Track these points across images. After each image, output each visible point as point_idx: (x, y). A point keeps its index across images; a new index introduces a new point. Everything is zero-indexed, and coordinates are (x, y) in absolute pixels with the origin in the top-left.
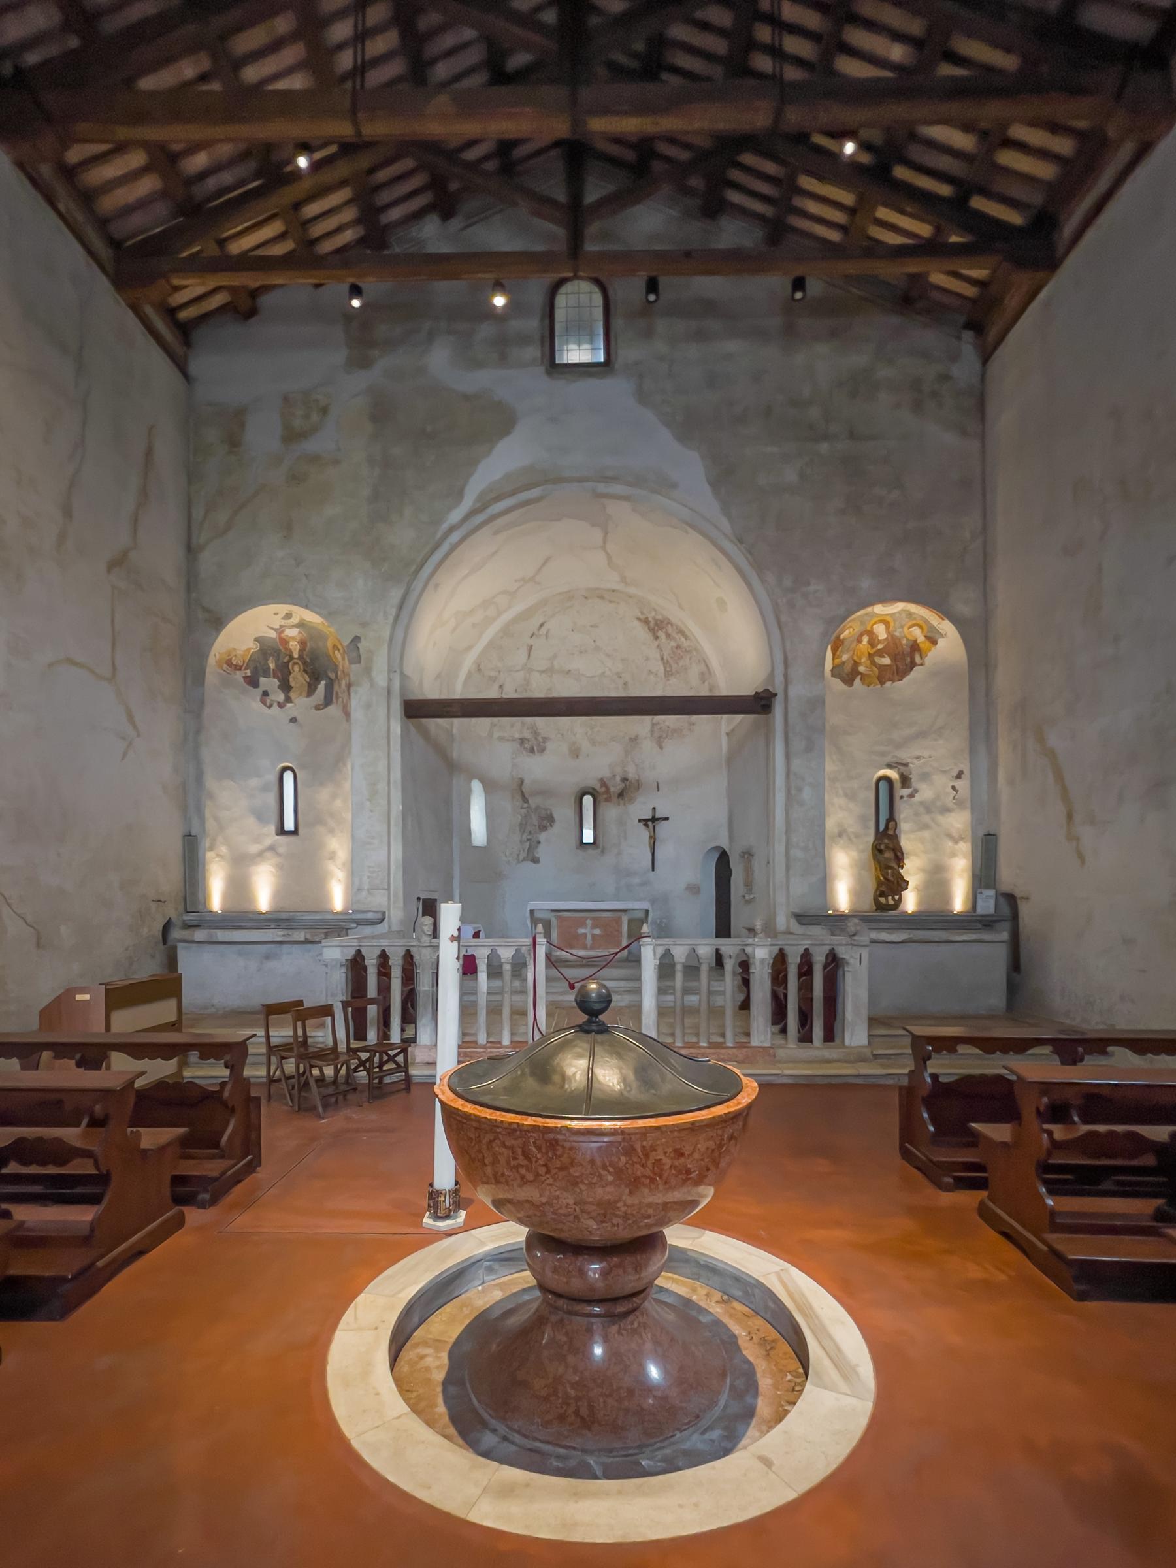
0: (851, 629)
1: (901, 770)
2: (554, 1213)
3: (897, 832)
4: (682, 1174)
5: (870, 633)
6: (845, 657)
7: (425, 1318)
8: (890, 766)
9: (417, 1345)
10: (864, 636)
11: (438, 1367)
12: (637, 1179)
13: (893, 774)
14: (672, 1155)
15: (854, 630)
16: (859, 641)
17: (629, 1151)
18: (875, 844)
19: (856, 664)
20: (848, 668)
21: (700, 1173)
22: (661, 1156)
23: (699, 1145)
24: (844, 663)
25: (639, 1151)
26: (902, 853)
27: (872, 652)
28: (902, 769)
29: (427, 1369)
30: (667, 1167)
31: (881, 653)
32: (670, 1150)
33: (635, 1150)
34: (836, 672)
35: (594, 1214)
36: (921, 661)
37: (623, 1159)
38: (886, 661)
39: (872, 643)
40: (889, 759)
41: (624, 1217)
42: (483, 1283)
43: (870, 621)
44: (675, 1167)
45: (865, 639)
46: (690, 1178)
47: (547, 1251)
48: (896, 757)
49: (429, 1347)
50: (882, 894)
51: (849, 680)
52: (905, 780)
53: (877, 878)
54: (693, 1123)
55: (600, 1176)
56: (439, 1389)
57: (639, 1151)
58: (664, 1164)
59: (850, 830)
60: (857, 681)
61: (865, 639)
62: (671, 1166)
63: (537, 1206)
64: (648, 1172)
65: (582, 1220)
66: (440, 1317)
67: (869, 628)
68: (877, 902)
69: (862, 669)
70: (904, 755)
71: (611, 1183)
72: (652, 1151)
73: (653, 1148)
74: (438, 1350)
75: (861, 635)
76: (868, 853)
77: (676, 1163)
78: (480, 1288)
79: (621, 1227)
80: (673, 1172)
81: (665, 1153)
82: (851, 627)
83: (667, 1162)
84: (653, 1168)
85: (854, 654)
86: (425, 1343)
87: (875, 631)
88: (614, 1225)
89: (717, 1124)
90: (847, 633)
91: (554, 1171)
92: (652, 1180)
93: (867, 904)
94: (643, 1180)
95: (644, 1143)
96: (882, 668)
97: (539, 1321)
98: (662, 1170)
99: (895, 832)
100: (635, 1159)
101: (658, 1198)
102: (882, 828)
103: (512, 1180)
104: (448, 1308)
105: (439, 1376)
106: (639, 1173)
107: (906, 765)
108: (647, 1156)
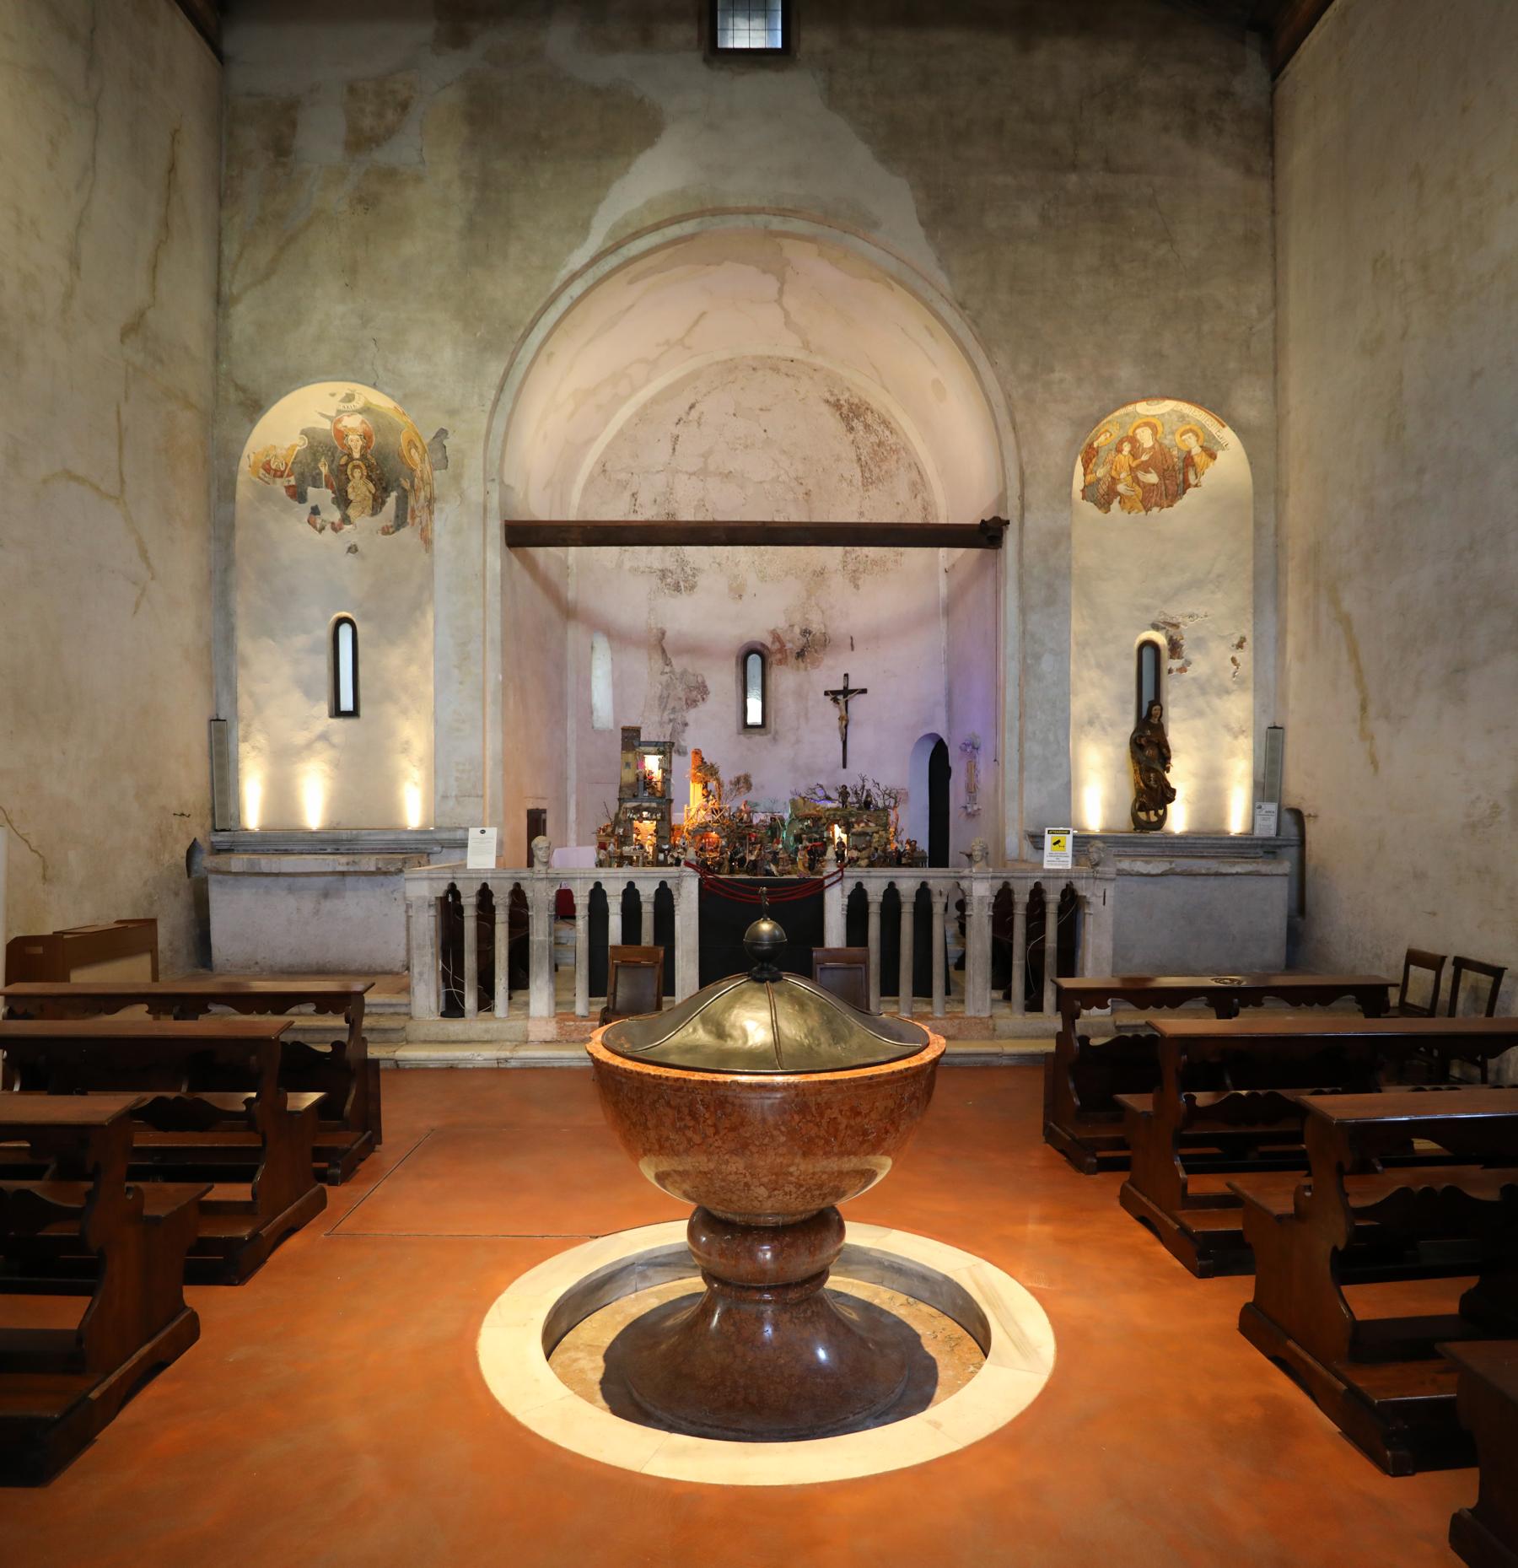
0: (1108, 435)
1: (1170, 633)
2: (723, 1180)
3: (1163, 720)
4: (858, 1135)
5: (1133, 440)
6: (1100, 473)
7: (574, 1324)
8: (1155, 627)
9: (568, 1349)
10: (1126, 444)
11: (593, 1369)
12: (811, 1140)
13: (1160, 638)
14: (848, 1114)
15: (1111, 435)
16: (1119, 450)
17: (803, 1109)
18: (1134, 736)
19: (1114, 481)
20: (1103, 488)
21: (878, 1136)
22: (835, 1113)
23: (877, 1104)
24: (1099, 480)
25: (814, 1109)
26: (1169, 751)
27: (1134, 465)
28: (1172, 631)
29: (582, 1371)
30: (843, 1126)
31: (1145, 468)
32: (846, 1108)
33: (808, 1107)
34: (1087, 492)
35: (765, 1180)
36: (1196, 482)
37: (797, 1118)
38: (1152, 478)
39: (1134, 454)
40: (1155, 616)
41: (796, 1183)
42: (636, 1291)
43: (1132, 423)
44: (851, 1127)
45: (1127, 448)
46: (868, 1140)
47: (713, 1232)
48: (1165, 614)
49: (581, 1351)
50: (1141, 809)
51: (1104, 503)
52: (1175, 647)
53: (1137, 783)
54: (871, 1078)
55: (772, 1137)
56: (597, 1387)
57: (814, 1109)
58: (839, 1124)
59: (1104, 716)
60: (1115, 505)
61: (1127, 448)
62: (847, 1127)
63: (705, 1173)
64: (822, 1133)
65: (752, 1188)
66: (590, 1324)
67: (1131, 434)
68: (1135, 818)
69: (1121, 488)
70: (1175, 612)
71: (783, 1144)
72: (827, 1109)
73: (828, 1105)
74: (591, 1354)
75: (1121, 442)
76: (1125, 750)
77: (853, 1123)
78: (633, 1296)
79: (794, 1196)
80: (849, 1132)
81: (841, 1111)
82: (1107, 431)
83: (844, 1122)
84: (828, 1128)
85: (1111, 468)
86: (577, 1348)
87: (1138, 437)
88: (786, 1194)
89: (898, 1080)
90: (1102, 438)
91: (722, 1132)
92: (827, 1142)
93: (1124, 821)
94: (817, 1140)
95: (819, 1100)
96: (1148, 489)
97: (706, 1312)
98: (837, 1130)
99: (1159, 720)
100: (809, 1118)
101: (833, 1164)
102: (1144, 713)
103: (678, 1144)
104: (597, 1315)
105: (599, 1375)
106: (813, 1133)
107: (1176, 626)
108: (822, 1115)
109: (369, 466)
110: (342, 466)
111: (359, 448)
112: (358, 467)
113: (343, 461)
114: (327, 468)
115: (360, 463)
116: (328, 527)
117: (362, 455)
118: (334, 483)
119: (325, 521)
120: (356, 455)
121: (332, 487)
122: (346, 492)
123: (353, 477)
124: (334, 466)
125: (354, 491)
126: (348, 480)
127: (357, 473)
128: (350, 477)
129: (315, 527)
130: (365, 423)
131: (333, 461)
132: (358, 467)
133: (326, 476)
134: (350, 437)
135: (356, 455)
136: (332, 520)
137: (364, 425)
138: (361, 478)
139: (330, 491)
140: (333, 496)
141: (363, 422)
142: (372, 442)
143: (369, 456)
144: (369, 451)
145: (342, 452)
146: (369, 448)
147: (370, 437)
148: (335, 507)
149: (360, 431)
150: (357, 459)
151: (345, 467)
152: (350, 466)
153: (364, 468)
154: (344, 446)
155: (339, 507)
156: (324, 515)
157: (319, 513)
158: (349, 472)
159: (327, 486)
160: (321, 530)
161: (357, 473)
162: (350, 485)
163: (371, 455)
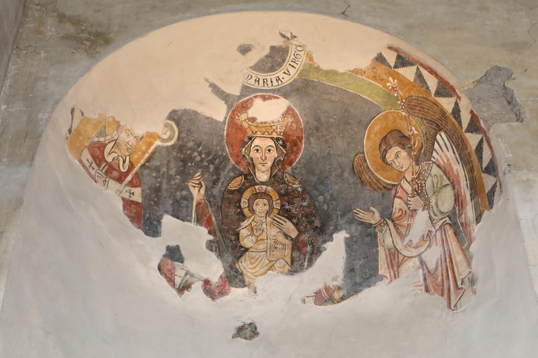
109: (287, 194)
110: (232, 192)
111: (270, 164)
112: (265, 195)
113: (235, 185)
114: (203, 191)
115: (269, 188)
116: (197, 287)
117: (273, 177)
118: (213, 219)
119: (192, 276)
120: (262, 176)
121: (208, 223)
122: (237, 234)
123: (253, 212)
124: (215, 191)
125: (252, 234)
126: (242, 217)
127: (261, 206)
128: (246, 211)
129: (171, 281)
130: (294, 115)
131: (215, 182)
132: (265, 195)
133: (198, 204)
134: (257, 142)
135: (262, 176)
136: (205, 276)
137: (290, 119)
138: (268, 213)
139: (204, 230)
140: (211, 238)
141: (289, 111)
142: (297, 153)
143: (288, 178)
144: (289, 169)
145: (234, 169)
146: (290, 164)
147: (296, 144)
148: (213, 256)
149: (280, 129)
150: (262, 183)
151: (236, 197)
152: (247, 194)
153: (275, 196)
154: (240, 158)
155: (220, 255)
156: (190, 265)
157: (181, 260)
158: (244, 204)
159: (199, 221)
160: (184, 288)
161: (261, 206)
162: (245, 223)
163: (293, 175)
